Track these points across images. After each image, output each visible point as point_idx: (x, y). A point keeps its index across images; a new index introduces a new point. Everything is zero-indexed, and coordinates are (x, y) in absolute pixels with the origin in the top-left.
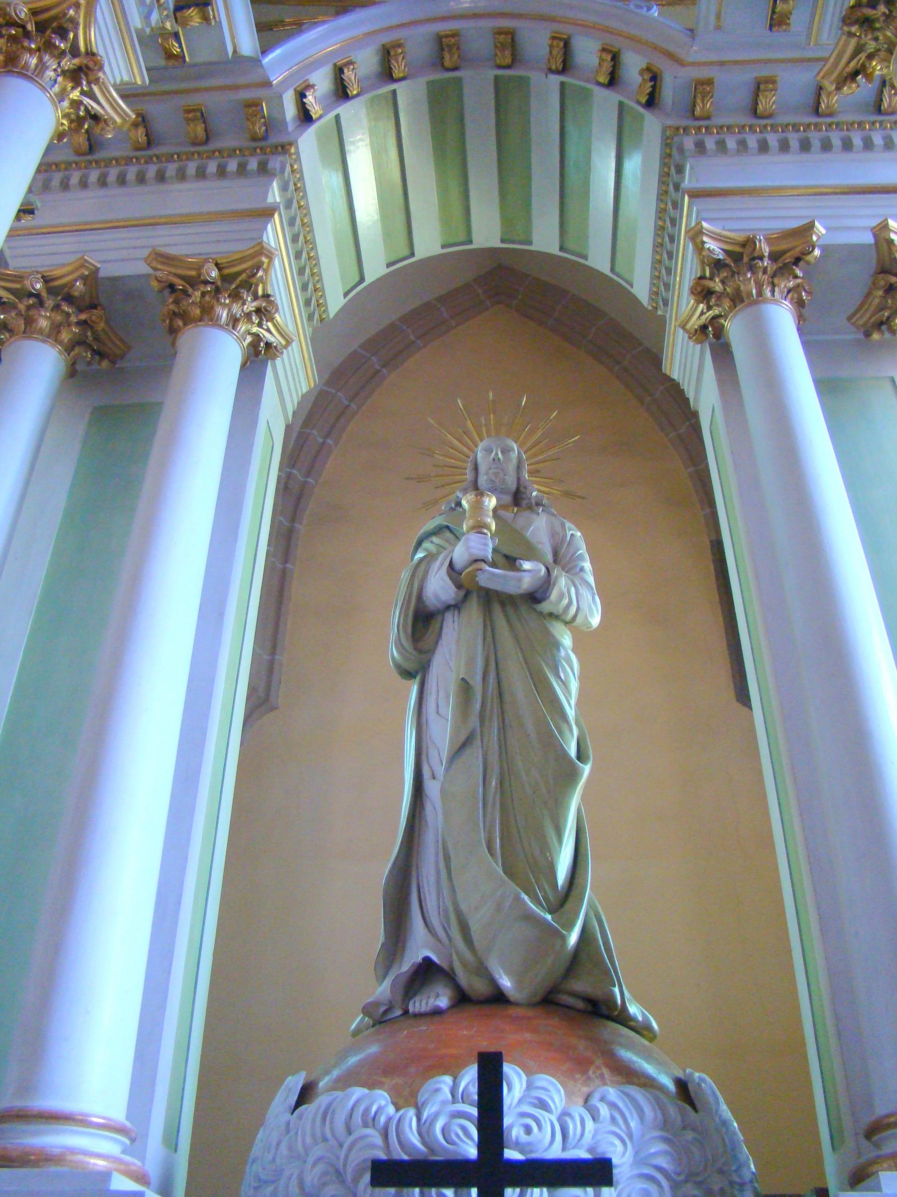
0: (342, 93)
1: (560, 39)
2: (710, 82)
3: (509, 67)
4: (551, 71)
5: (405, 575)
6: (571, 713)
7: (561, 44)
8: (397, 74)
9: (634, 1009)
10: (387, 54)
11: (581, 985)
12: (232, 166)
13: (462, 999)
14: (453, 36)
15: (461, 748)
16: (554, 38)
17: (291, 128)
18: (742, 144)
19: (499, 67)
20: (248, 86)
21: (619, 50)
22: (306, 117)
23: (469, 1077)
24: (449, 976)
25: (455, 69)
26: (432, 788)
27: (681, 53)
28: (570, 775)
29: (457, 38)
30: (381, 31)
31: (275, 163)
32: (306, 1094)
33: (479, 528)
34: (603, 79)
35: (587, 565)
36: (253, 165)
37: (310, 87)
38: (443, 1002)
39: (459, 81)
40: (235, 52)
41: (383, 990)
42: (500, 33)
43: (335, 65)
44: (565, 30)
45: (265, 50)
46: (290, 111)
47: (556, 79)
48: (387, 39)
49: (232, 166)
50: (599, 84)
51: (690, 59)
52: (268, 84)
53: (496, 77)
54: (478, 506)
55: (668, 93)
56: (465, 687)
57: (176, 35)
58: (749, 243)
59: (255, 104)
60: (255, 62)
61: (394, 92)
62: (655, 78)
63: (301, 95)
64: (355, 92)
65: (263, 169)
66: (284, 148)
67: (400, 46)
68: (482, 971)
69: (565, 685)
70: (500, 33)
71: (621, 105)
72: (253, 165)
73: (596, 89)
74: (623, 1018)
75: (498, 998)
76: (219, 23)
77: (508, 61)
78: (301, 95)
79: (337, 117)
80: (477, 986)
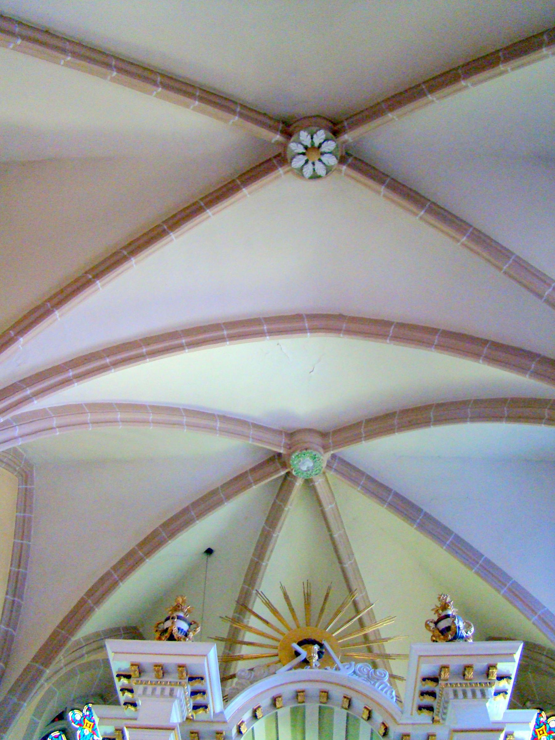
0: (255, 716)
1: (348, 698)
2: (408, 735)
3: (326, 703)
4: (342, 707)
7: (348, 701)
8: (278, 706)
10: (274, 700)
14: (303, 691)
16: (345, 697)
17: (233, 738)
19: (321, 702)
20: (218, 722)
21: (372, 710)
22: (240, 732)
25: (303, 702)
27: (397, 718)
29: (304, 693)
30: (273, 688)
34: (365, 716)
37: (243, 722)
39: (304, 706)
40: (214, 712)
42: (322, 692)
43: (253, 709)
44: (350, 694)
45: (225, 708)
46: (234, 731)
47: (346, 711)
48: (274, 693)
50: (364, 719)
51: (400, 722)
52: (225, 722)
53: (320, 708)
55: (391, 733)
57: (192, 716)
59: (219, 733)
60: (222, 713)
61: (277, 713)
62: (386, 729)
63: (239, 727)
64: (261, 716)
67: (280, 697)
70: (322, 692)
73: (362, 720)
76: (210, 711)
77: (325, 700)
78: (239, 727)
79: (253, 729)
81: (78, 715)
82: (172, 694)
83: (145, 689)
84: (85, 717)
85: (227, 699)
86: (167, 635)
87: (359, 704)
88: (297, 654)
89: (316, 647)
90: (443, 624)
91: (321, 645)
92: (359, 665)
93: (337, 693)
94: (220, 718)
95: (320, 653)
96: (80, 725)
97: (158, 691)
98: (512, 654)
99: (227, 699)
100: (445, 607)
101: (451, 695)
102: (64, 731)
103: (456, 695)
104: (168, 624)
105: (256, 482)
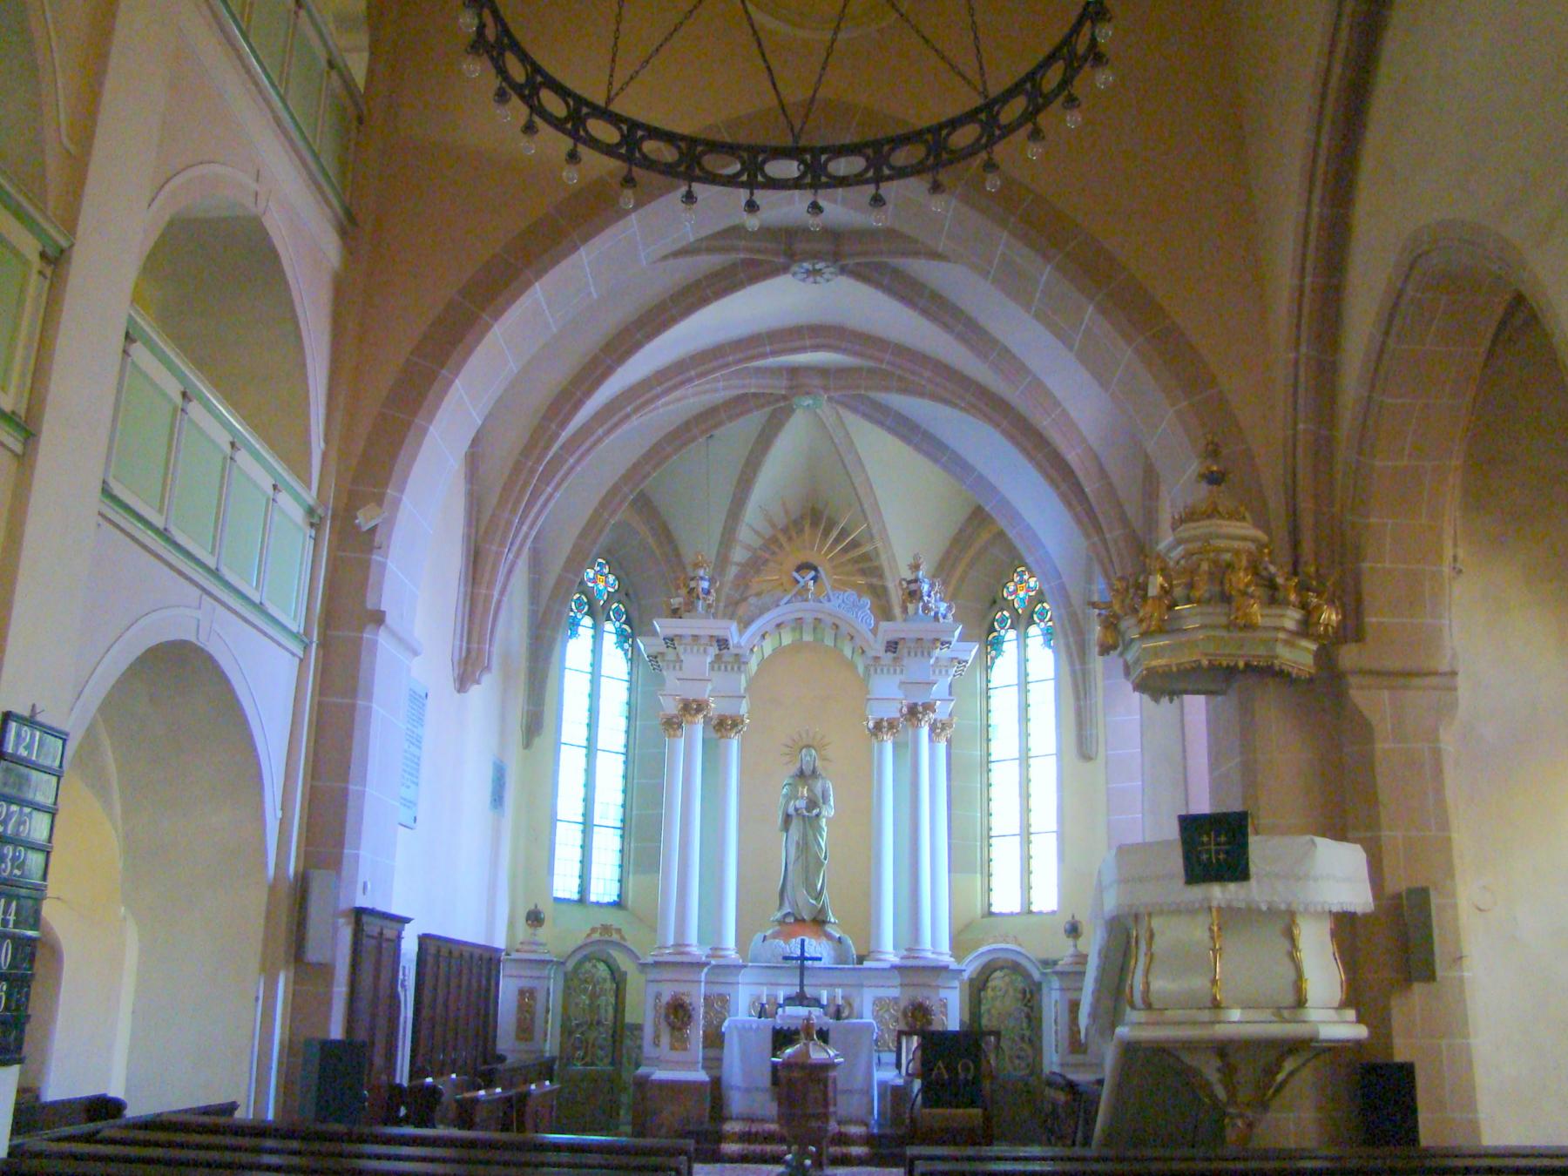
5: (782, 801)
6: (823, 844)
9: (832, 920)
11: (820, 918)
12: (729, 668)
13: (796, 920)
15: (797, 859)
18: (888, 670)
22: (752, 650)
23: (799, 940)
24: (793, 914)
26: (790, 867)
28: (822, 864)
31: (742, 669)
32: (765, 938)
33: (802, 797)
35: (832, 799)
36: (736, 668)
38: (792, 920)
41: (779, 915)
49: (729, 668)
54: (802, 792)
56: (798, 843)
58: (882, 720)
60: (738, 642)
65: (739, 668)
66: (746, 663)
68: (800, 914)
69: (821, 836)
71: (853, 649)
72: (736, 668)
74: (830, 922)
75: (803, 920)
80: (799, 918)
81: (591, 573)
82: (705, 651)
83: (685, 650)
84: (596, 573)
85: (741, 633)
86: (695, 595)
87: (844, 628)
88: (798, 582)
89: (812, 573)
90: (913, 587)
91: (816, 569)
92: (846, 594)
93: (829, 620)
94: (738, 646)
95: (815, 579)
96: (595, 582)
97: (695, 649)
98: (954, 632)
99: (741, 633)
100: (915, 567)
101: (906, 654)
102: (582, 592)
103: (909, 653)
104: (693, 584)
105: (758, 408)
